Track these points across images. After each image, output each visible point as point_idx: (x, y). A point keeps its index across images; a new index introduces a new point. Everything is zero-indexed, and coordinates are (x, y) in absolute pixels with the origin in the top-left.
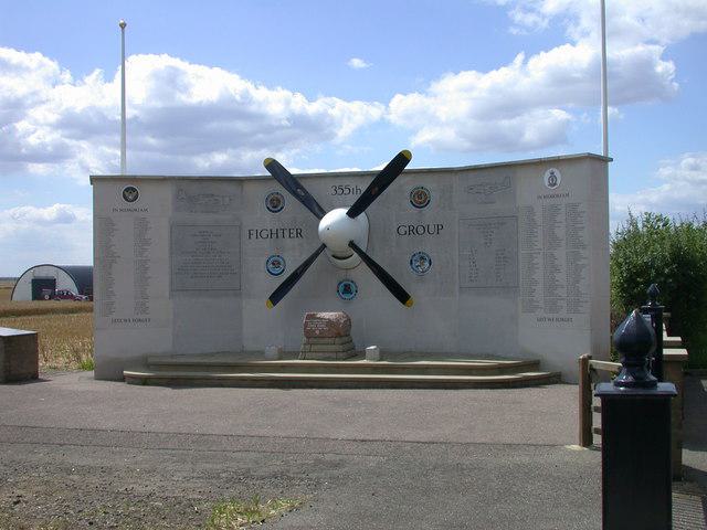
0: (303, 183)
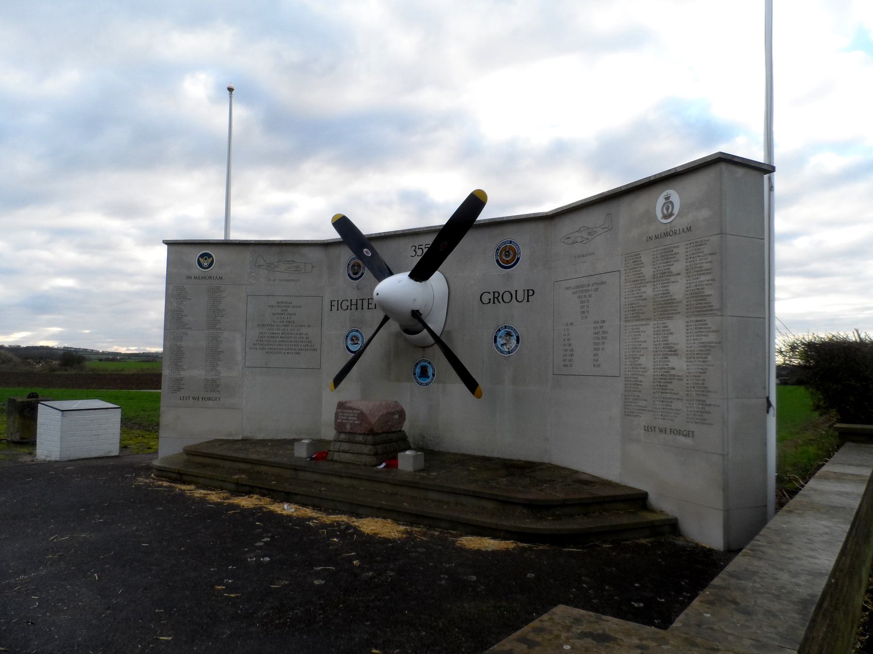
0: (375, 245)
